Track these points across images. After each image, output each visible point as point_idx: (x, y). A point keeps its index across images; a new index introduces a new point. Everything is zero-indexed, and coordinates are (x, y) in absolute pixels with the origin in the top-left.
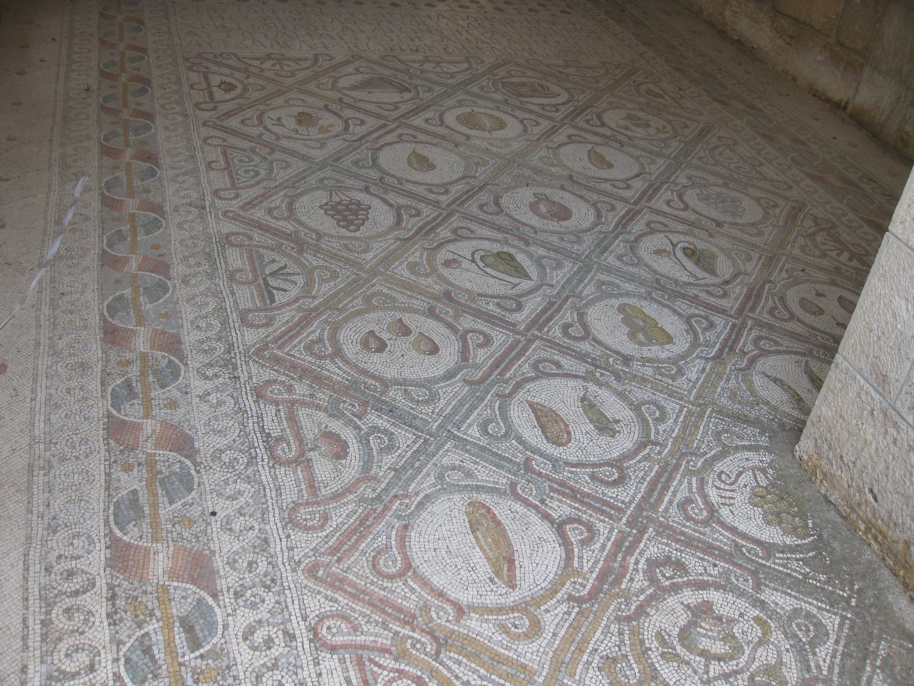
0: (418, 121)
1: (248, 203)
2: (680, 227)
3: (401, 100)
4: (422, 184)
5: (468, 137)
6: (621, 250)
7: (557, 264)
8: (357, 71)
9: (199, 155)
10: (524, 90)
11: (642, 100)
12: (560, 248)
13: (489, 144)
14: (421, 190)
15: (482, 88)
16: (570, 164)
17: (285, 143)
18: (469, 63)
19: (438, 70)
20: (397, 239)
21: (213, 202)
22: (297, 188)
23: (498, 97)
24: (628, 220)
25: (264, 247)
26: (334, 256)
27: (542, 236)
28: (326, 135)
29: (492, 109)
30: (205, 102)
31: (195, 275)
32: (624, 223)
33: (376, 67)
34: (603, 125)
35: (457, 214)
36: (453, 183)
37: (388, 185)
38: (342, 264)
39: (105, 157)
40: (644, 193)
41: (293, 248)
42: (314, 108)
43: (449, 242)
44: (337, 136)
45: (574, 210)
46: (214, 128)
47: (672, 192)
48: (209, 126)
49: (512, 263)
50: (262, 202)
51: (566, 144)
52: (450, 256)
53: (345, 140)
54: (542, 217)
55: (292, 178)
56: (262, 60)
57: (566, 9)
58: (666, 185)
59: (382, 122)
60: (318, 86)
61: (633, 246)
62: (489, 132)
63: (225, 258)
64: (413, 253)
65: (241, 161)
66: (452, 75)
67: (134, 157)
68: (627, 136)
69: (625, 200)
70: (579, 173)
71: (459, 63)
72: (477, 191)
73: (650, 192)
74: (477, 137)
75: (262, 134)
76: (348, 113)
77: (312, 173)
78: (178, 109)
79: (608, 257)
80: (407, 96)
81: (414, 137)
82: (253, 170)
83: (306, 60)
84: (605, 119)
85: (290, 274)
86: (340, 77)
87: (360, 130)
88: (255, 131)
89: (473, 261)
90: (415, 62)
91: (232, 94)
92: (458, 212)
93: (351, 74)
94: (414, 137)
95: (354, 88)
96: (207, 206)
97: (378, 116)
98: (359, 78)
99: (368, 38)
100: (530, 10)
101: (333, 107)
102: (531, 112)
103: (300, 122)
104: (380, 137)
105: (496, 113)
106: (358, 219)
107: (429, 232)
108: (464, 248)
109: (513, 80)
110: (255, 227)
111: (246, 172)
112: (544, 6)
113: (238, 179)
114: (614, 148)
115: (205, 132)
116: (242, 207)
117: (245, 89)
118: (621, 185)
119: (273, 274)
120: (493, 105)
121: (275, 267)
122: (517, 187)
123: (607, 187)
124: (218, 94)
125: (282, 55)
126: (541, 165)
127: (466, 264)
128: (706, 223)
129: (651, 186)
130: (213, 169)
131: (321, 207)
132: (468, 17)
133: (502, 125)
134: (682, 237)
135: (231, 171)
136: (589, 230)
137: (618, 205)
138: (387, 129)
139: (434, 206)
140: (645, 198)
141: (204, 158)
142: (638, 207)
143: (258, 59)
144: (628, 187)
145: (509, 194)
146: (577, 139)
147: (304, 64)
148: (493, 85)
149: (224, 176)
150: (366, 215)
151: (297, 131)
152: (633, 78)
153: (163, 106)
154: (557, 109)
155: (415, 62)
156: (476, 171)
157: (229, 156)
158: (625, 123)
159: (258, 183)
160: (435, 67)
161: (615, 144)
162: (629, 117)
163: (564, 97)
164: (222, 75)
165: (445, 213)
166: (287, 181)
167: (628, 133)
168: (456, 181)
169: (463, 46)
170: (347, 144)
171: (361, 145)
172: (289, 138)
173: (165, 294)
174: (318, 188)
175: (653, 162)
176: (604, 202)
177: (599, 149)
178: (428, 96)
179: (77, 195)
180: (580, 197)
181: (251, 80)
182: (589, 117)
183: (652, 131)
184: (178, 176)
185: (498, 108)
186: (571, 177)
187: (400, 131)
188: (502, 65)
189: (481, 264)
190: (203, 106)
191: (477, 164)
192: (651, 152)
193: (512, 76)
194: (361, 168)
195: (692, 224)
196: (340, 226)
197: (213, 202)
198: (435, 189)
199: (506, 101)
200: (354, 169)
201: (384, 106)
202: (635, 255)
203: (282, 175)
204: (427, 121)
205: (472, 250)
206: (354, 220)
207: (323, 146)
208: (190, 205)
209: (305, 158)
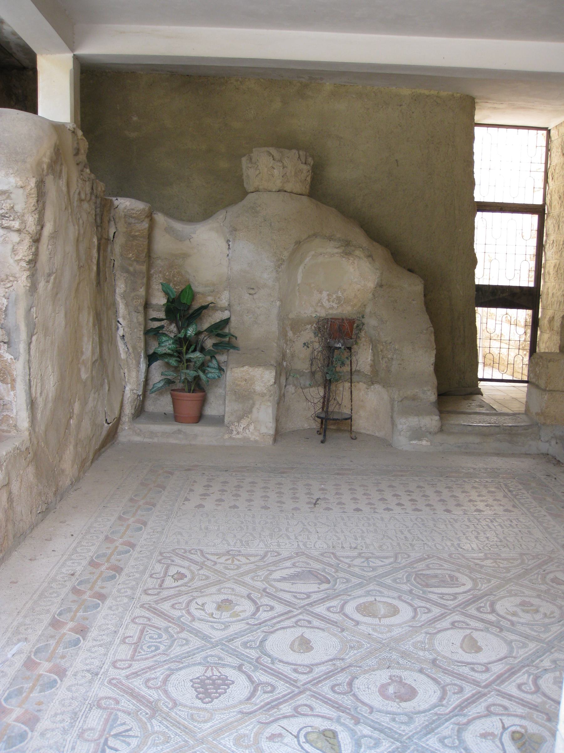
0: (320, 609)
1: (133, 673)
2: (520, 710)
3: (317, 590)
5: (357, 623)
6: (447, 732)
7: (375, 744)
8: (294, 565)
9: (121, 631)
11: (544, 587)
12: (387, 728)
13: (374, 629)
15: (395, 581)
16: (439, 649)
17: (197, 625)
19: (365, 564)
20: (241, 712)
21: (107, 670)
22: (182, 663)
23: (406, 587)
24: (469, 703)
25: (124, 712)
26: (177, 724)
27: (375, 716)
28: (235, 619)
29: (394, 598)
30: (153, 589)
31: (53, 730)
32: (462, 707)
33: (311, 562)
34: (493, 611)
35: (308, 693)
36: (320, 664)
37: (261, 664)
38: (178, 731)
39: (50, 628)
40: (498, 677)
41: (147, 714)
42: (238, 596)
43: (285, 717)
44: (243, 620)
45: (420, 692)
46: (148, 609)
47: (529, 676)
48: (145, 608)
49: (332, 741)
50: (146, 672)
51: (448, 629)
52: (278, 730)
53: (248, 624)
54: (385, 697)
55: (183, 654)
56: (219, 555)
57: (511, 508)
58: (524, 670)
60: (252, 579)
61: (461, 729)
62: (380, 619)
63: (86, 717)
64: (246, 726)
65: (151, 638)
66: (374, 569)
67: (71, 630)
68: (509, 620)
69: (476, 683)
70: (444, 657)
71: (386, 558)
72: (338, 672)
73: (506, 675)
74: (365, 623)
75: (182, 616)
77: (203, 650)
78: (129, 592)
79: (430, 738)
80: (325, 586)
81: (309, 622)
82: (154, 646)
83: (257, 555)
84: (498, 607)
85: (129, 736)
86: (275, 571)
87: (263, 615)
88: (176, 613)
89: (297, 737)
90: (347, 557)
91: (180, 582)
92: (310, 690)
93: (286, 568)
95: (283, 579)
96: (101, 673)
97: (288, 603)
98: (292, 571)
99: (319, 538)
101: (254, 595)
102: (428, 600)
104: (279, 622)
105: (396, 602)
106: (216, 693)
107: (273, 707)
108: (294, 725)
110: (127, 693)
111: (149, 647)
113: (140, 652)
114: (492, 633)
115: (138, 612)
116: (127, 677)
117: (192, 579)
118: (480, 668)
119: (116, 736)
120: (396, 595)
121: (122, 729)
122: (378, 669)
123: (465, 670)
125: (240, 551)
126: (411, 649)
127: (289, 739)
128: (550, 706)
129: (509, 670)
130: (125, 643)
131: (191, 681)
132: (416, 519)
133: (395, 611)
134: (517, 721)
135: (138, 646)
136: (424, 712)
137: (467, 688)
138: (290, 615)
139: (291, 684)
140: (498, 682)
141: (124, 634)
142: (486, 690)
143: (217, 554)
144: (487, 670)
145: (367, 676)
146: (460, 625)
147: (252, 559)
148: (407, 578)
149: (129, 649)
150: (225, 689)
152: (544, 567)
153: (119, 591)
154: (455, 596)
155: (347, 557)
157: (145, 633)
158: (515, 609)
159: (152, 657)
161: (495, 629)
162: (523, 604)
163: (469, 585)
164: (181, 567)
165: (297, 691)
166: (177, 656)
167: (514, 619)
168: (323, 663)
169: (399, 544)
170: (248, 627)
171: (259, 628)
172: (202, 620)
173: (21, 742)
174: (200, 664)
175: (525, 646)
176: (455, 685)
177: (475, 634)
178: (343, 587)
179: (9, 656)
180: (434, 679)
181: (201, 572)
182: (482, 605)
183: (538, 617)
184: (94, 647)
185: (399, 598)
186: (434, 661)
187: (301, 617)
189: (302, 739)
190: (150, 592)
191: (351, 647)
192: (527, 637)
194: (247, 648)
195: (535, 707)
196: (197, 697)
197: (107, 670)
198: (300, 669)
199: (411, 591)
200: (241, 649)
201: (298, 595)
202: (459, 737)
203: (177, 650)
204: (328, 609)
205: (302, 725)
206: (212, 693)
207: (227, 627)
208: (88, 671)
209: (205, 638)
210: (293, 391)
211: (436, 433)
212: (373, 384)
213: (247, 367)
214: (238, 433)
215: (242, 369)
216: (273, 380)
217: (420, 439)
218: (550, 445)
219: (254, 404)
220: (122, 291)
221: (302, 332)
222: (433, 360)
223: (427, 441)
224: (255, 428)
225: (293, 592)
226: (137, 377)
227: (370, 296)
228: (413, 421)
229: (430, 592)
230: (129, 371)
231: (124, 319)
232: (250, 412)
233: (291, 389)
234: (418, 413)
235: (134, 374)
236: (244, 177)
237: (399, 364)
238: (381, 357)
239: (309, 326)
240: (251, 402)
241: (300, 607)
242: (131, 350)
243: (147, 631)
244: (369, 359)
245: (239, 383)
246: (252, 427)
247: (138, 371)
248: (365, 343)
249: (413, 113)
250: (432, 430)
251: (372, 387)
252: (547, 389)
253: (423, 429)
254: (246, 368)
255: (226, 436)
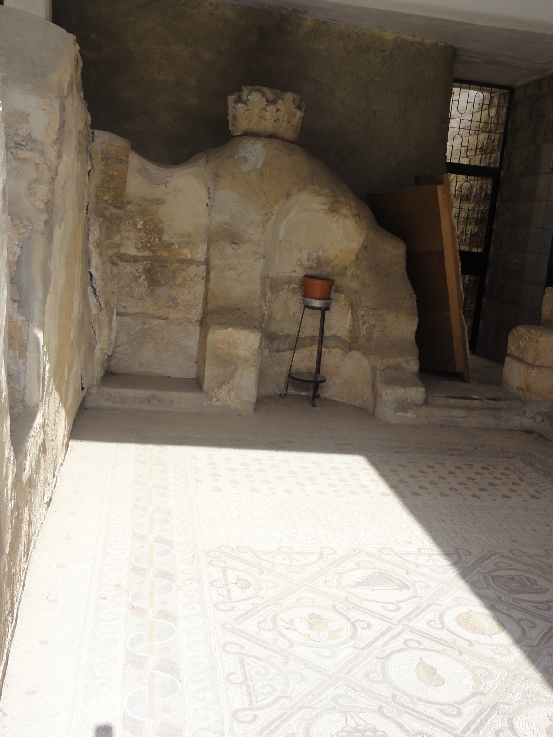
0: (420, 623)
4: (433, 703)
10: (514, 585)
14: (433, 711)
18: (459, 555)
36: (464, 702)
59: (388, 625)
62: (490, 635)
76: (355, 615)
80: (406, 594)
94: (418, 642)
95: (359, 584)
100: (504, 496)
103: (311, 626)
104: (387, 643)
109: (502, 573)
112: (515, 491)
124: (237, 593)
151: (309, 636)
156: (485, 686)
160: (428, 561)
188: (489, 557)
190: (222, 606)
193: (500, 569)
210: (267, 355)
211: (421, 406)
212: (350, 350)
213: (231, 329)
214: (218, 400)
215: (225, 331)
216: (257, 344)
217: (406, 412)
218: (535, 421)
219: (236, 370)
220: (96, 238)
221: (280, 293)
222: (415, 328)
223: (413, 414)
224: (237, 395)
225: (381, 602)
226: (109, 336)
227: (353, 257)
228: (401, 392)
229: (519, 600)
230: (100, 328)
231: (97, 270)
232: (232, 377)
233: (266, 352)
234: (403, 382)
235: (105, 332)
236: (230, 118)
237: (381, 331)
238: (361, 322)
239: (286, 286)
240: (233, 367)
241: (400, 622)
242: (103, 305)
243: (249, 664)
244: (348, 324)
245: (221, 346)
246: (233, 394)
247: (110, 329)
248: (344, 307)
249: (395, 60)
250: (417, 402)
251: (350, 353)
252: (536, 364)
253: (409, 401)
254: (230, 330)
255: (206, 403)
